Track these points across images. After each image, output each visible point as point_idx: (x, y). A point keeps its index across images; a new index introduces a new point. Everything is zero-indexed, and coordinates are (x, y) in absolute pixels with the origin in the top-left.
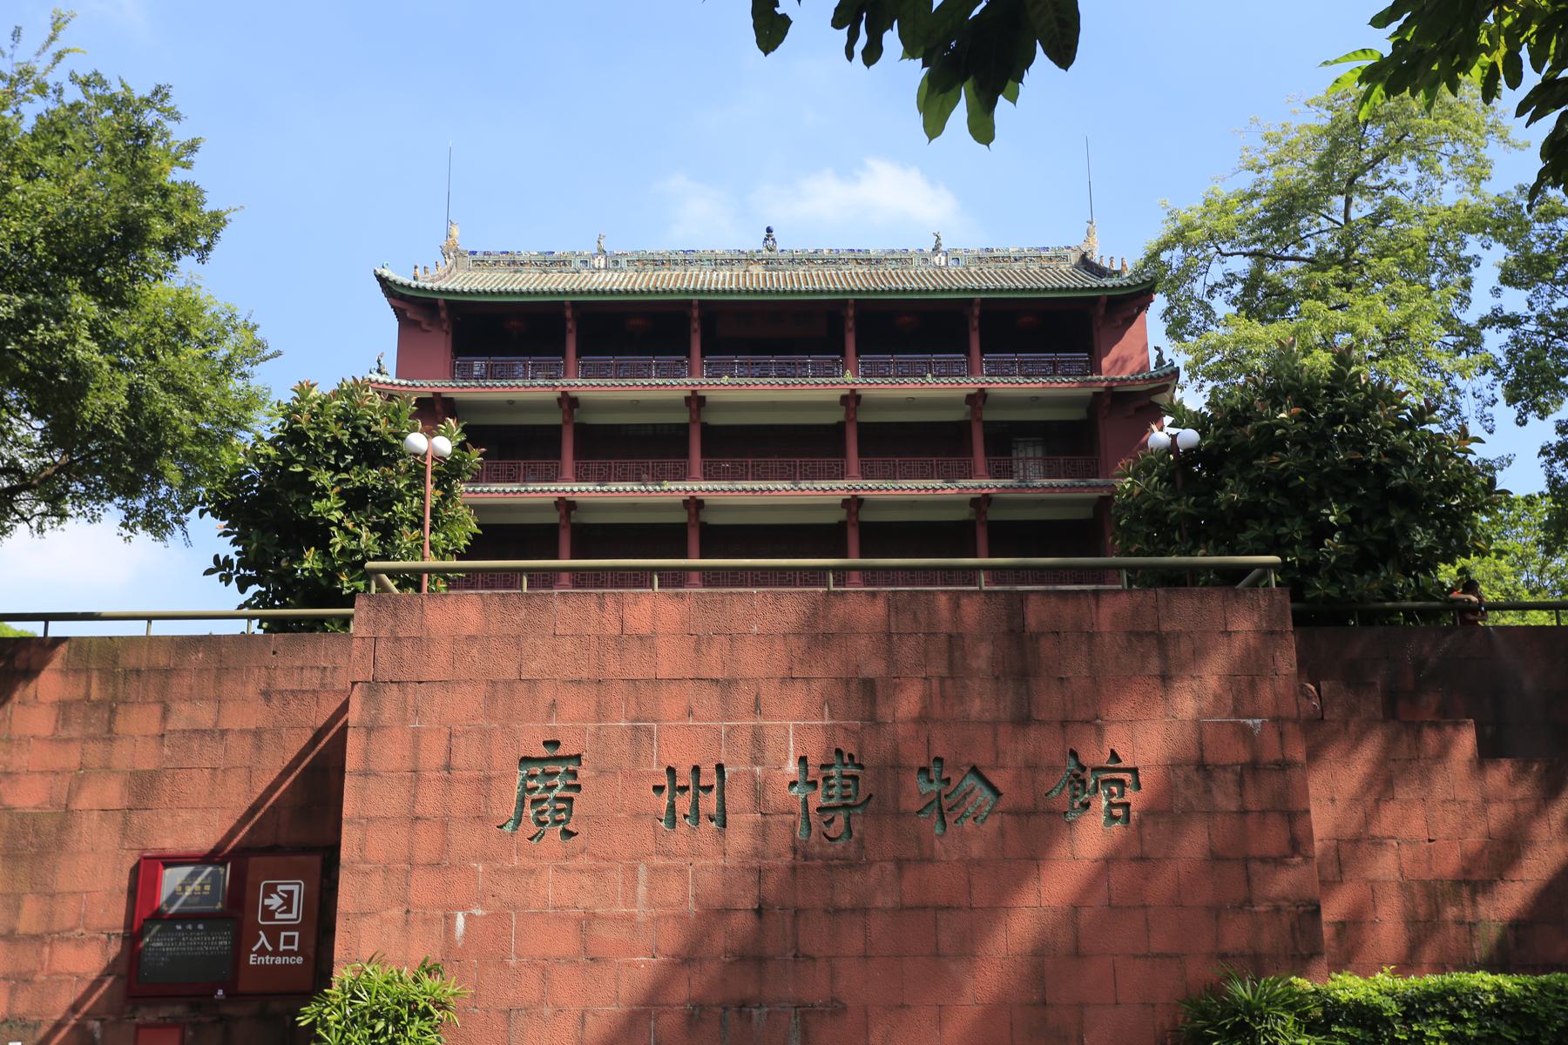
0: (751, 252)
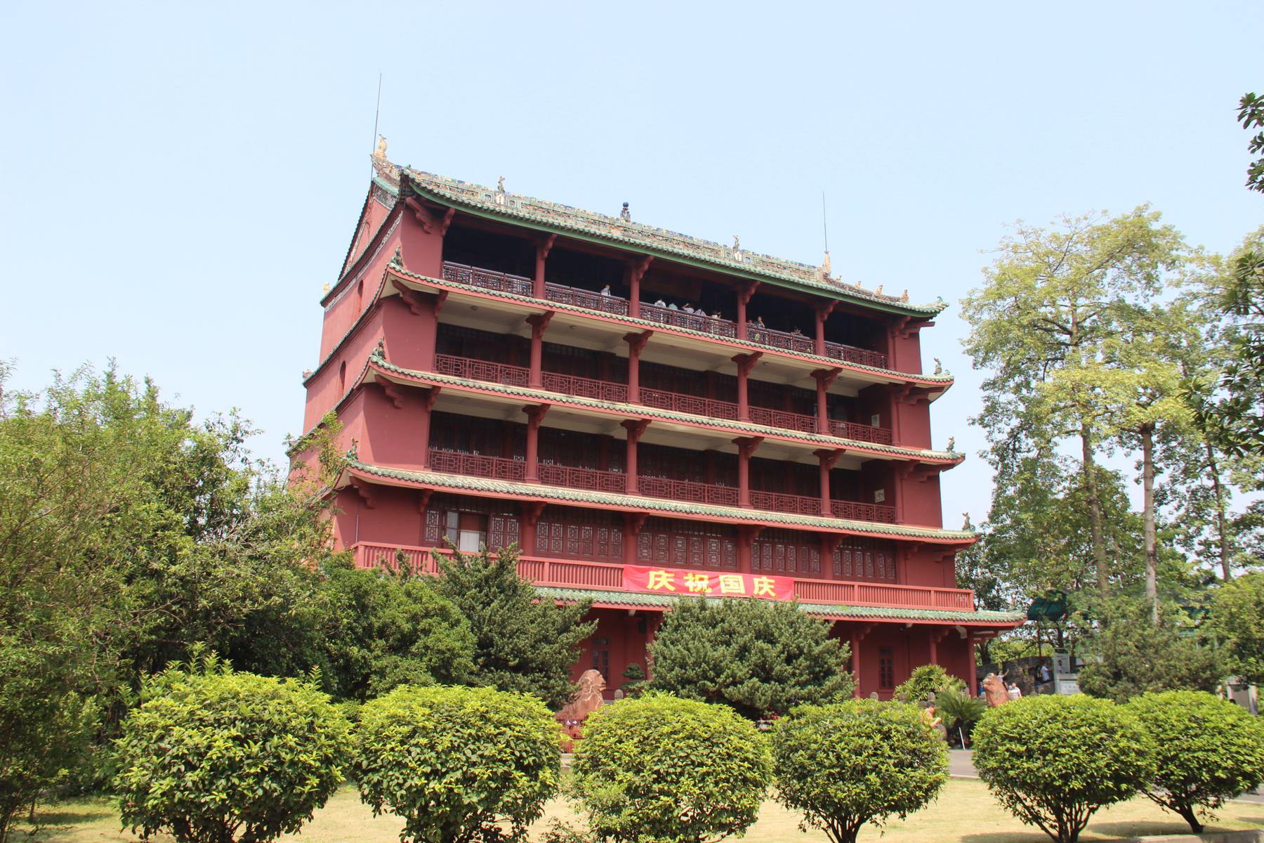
0: (612, 219)
